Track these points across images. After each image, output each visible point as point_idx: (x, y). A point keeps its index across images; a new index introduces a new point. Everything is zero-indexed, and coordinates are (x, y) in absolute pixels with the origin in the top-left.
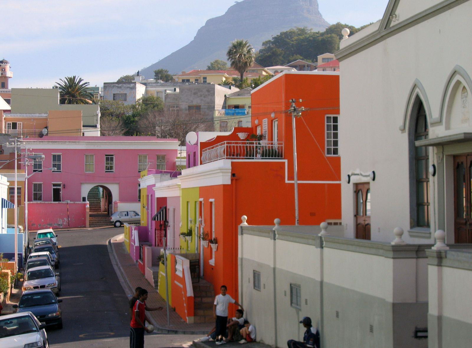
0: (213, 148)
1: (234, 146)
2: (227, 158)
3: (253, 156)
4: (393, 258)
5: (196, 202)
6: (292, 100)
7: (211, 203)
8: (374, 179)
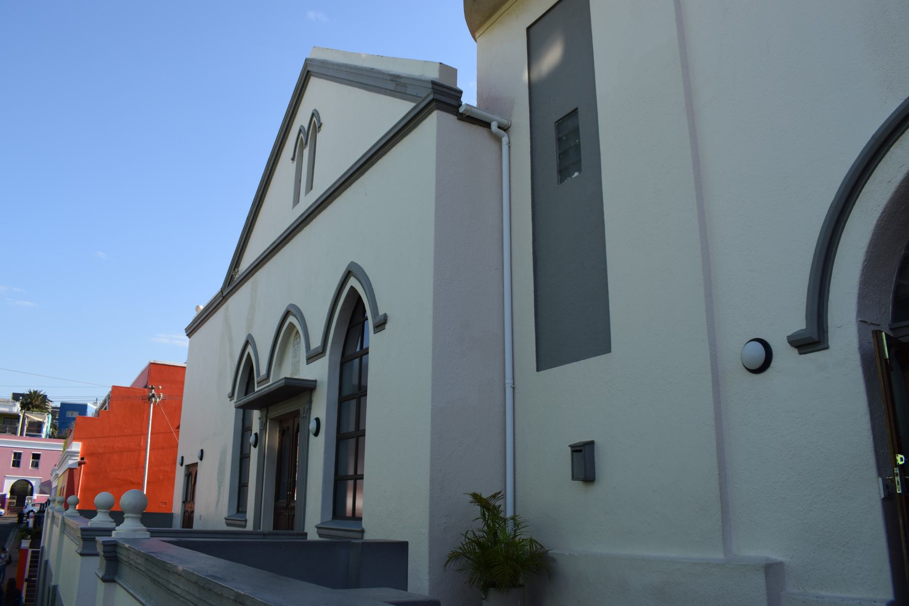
8: (201, 459)
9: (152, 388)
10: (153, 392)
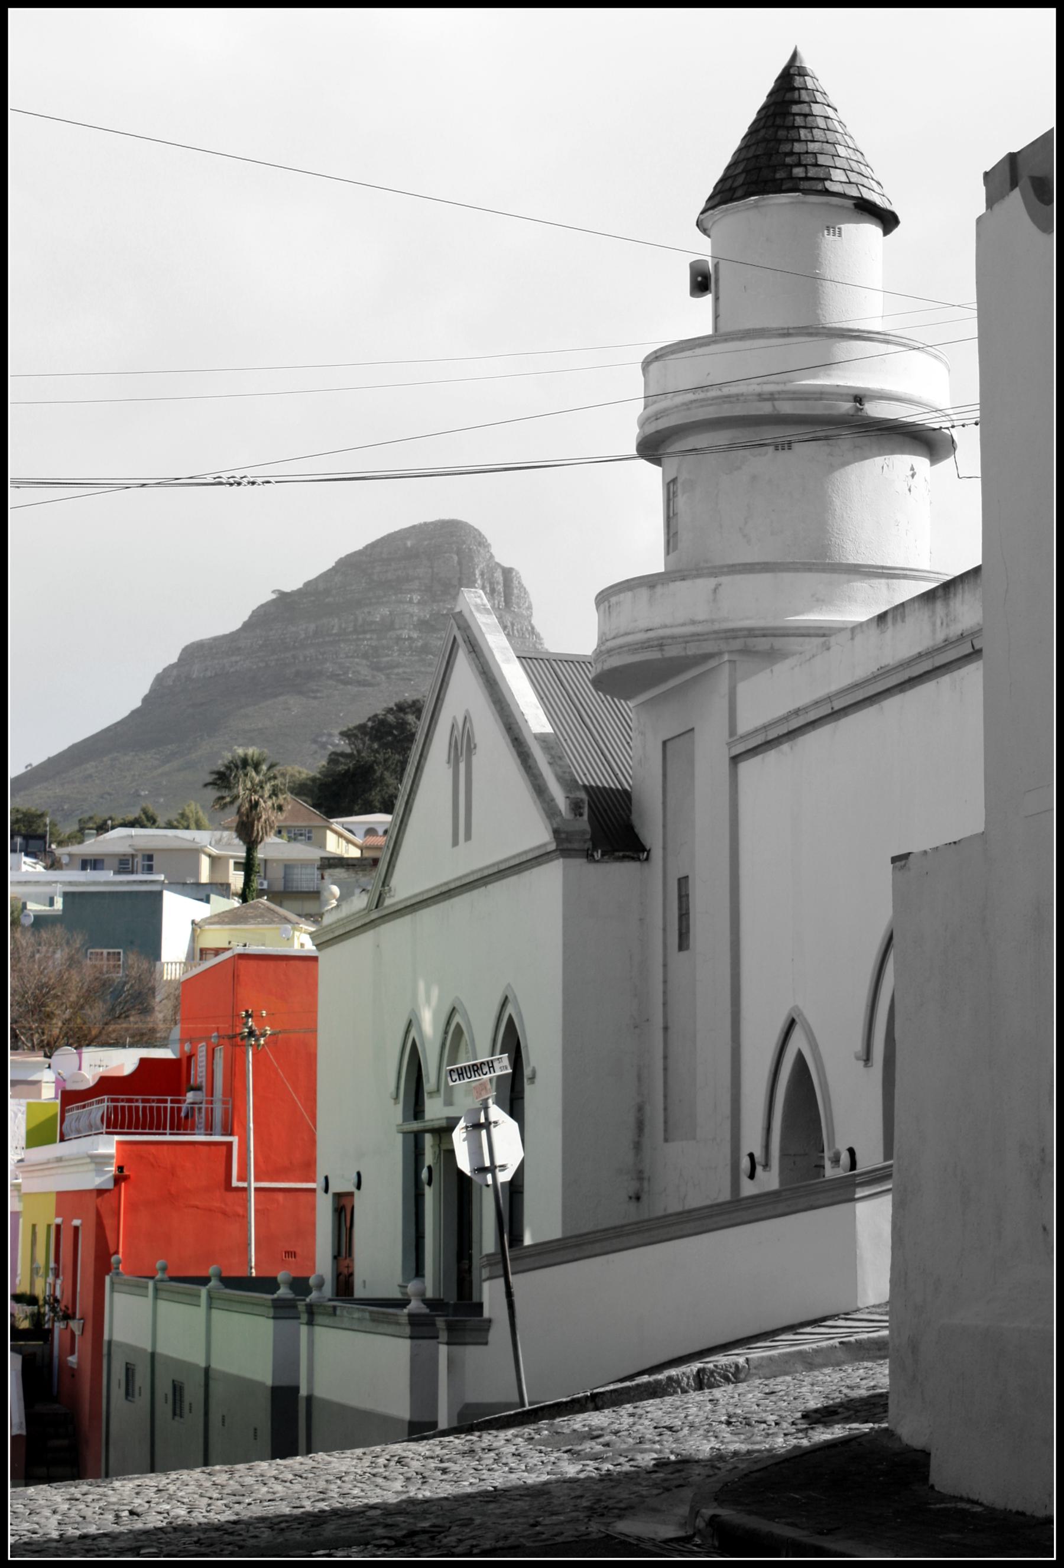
0: (84, 1107)
1: (123, 1107)
2: (108, 1133)
3: (165, 1128)
4: (274, 1318)
5: (49, 1226)
6: (247, 1012)
7: (76, 1229)
8: (359, 1187)
9: (248, 1016)
10: (250, 1024)
